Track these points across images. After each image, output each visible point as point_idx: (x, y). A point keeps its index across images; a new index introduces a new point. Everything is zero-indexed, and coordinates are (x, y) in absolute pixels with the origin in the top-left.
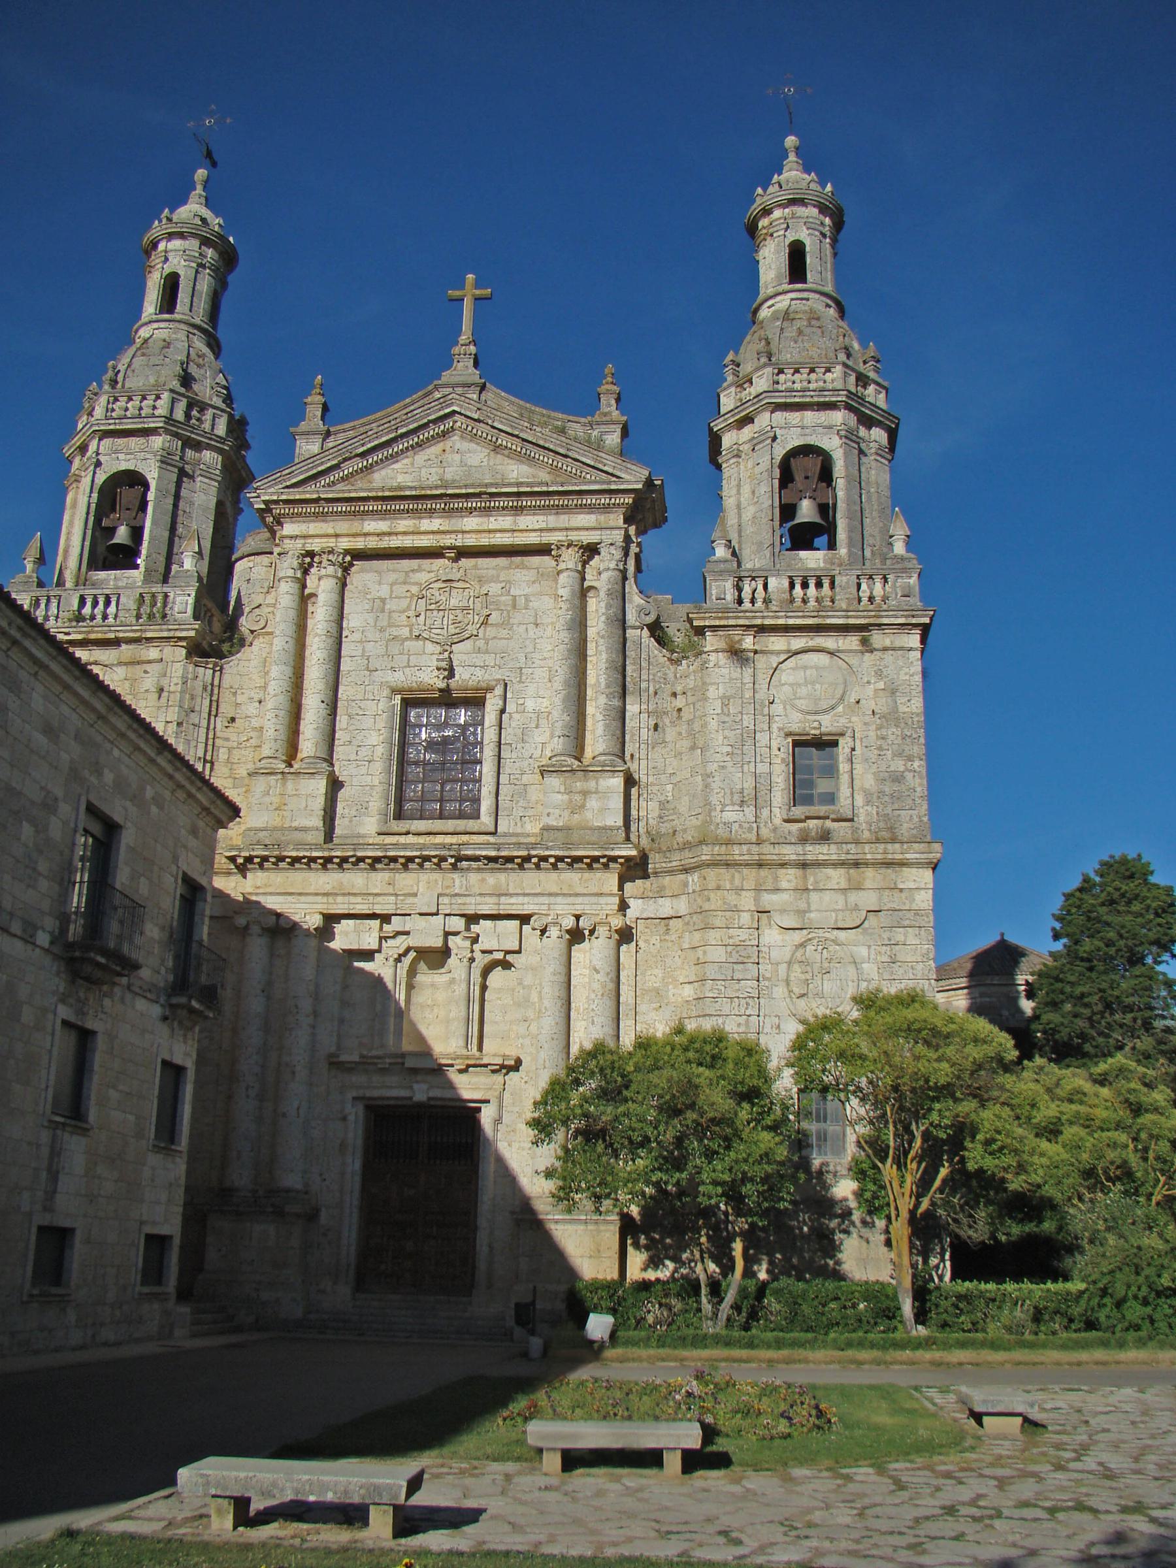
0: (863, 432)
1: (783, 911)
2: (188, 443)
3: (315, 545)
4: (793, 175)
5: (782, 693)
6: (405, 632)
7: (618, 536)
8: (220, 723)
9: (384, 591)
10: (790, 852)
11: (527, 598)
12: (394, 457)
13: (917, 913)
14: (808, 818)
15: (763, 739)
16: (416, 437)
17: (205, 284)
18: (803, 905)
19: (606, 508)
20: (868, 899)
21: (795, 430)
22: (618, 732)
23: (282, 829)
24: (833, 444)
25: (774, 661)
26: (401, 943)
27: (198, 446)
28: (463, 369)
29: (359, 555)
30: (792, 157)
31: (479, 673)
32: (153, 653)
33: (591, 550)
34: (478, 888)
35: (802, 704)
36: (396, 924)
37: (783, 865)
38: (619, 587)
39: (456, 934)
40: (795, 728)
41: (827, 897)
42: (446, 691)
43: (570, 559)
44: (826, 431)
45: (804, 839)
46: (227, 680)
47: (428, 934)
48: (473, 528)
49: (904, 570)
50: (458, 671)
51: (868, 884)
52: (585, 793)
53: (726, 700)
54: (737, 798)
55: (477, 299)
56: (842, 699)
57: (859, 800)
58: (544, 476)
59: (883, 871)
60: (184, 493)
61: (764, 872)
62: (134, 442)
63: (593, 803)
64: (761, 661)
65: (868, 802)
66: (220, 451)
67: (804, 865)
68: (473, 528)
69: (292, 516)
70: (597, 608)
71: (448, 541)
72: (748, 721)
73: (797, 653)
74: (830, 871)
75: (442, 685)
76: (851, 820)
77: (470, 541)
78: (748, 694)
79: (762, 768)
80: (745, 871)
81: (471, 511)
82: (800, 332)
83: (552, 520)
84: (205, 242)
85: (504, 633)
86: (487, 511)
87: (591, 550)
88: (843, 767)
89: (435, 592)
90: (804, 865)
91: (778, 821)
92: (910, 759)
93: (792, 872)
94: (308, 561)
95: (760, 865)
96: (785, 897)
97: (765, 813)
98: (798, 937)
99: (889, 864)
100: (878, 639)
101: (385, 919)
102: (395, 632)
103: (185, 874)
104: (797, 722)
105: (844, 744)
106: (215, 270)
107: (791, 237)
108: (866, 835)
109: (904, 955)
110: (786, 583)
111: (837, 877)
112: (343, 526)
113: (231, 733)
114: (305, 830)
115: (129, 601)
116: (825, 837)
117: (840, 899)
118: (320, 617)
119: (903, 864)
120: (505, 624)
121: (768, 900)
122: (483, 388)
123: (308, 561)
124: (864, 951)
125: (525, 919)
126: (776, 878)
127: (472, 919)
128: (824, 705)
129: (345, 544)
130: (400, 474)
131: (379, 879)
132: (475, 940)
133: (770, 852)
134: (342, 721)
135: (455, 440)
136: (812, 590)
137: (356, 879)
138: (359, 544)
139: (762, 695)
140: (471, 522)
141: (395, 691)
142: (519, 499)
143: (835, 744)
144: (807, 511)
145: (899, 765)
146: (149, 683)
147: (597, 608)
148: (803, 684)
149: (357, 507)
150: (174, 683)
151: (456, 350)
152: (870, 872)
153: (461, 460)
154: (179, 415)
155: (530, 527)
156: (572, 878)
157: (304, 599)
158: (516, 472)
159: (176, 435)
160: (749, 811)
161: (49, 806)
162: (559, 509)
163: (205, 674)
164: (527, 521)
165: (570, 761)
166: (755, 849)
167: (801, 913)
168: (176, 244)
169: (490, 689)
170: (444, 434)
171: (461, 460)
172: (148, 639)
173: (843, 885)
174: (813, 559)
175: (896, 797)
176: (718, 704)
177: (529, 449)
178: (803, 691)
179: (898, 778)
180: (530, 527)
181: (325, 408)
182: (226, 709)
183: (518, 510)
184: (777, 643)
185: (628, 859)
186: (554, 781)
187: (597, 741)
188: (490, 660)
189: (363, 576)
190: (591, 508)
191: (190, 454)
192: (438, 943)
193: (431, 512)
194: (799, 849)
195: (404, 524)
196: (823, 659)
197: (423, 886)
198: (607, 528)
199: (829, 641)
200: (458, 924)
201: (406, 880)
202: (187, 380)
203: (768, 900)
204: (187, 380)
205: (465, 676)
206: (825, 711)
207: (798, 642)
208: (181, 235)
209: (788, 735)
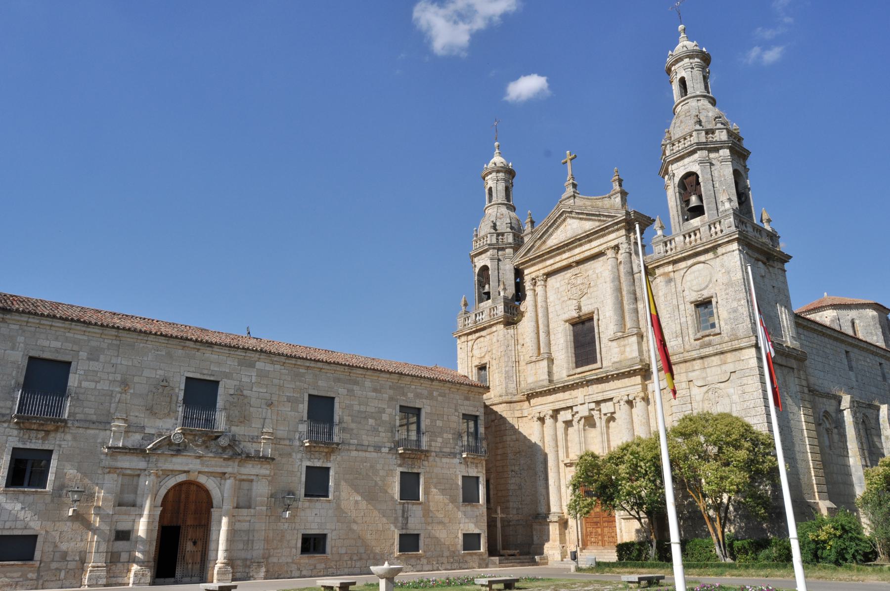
0: (712, 155)
1: (697, 379)
2: (499, 249)
3: (533, 275)
4: (685, 44)
5: (687, 285)
6: (566, 298)
7: (624, 239)
8: (519, 347)
9: (558, 285)
10: (695, 354)
11: (601, 273)
12: (551, 235)
13: (751, 369)
14: (703, 337)
15: (682, 307)
16: (554, 224)
17: (502, 186)
18: (704, 375)
19: (618, 230)
20: (730, 367)
21: (679, 170)
22: (635, 318)
23: (536, 382)
24: (696, 168)
25: (682, 272)
26: (577, 417)
27: (503, 249)
28: (570, 190)
29: (549, 275)
30: (683, 35)
31: (590, 306)
32: (494, 329)
33: (616, 248)
34: (596, 391)
35: (695, 288)
36: (575, 409)
37: (694, 360)
38: (628, 259)
39: (593, 409)
40: (693, 299)
41: (714, 369)
42: (579, 317)
43: (610, 253)
44: (691, 165)
45: (702, 347)
46: (520, 331)
47: (583, 411)
48: (579, 253)
49: (726, 216)
50: (583, 308)
51: (729, 360)
52: (624, 346)
53: (665, 296)
54: (674, 335)
55: (571, 160)
56: (710, 281)
57: (722, 323)
58: (597, 224)
59: (734, 353)
60: (501, 266)
61: (688, 364)
62: (483, 256)
63: (628, 349)
64: (678, 275)
65: (726, 324)
66: (511, 247)
67: (702, 358)
68: (579, 253)
69: (526, 268)
70: (622, 269)
71: (571, 260)
72: (675, 302)
73: (690, 267)
74: (713, 358)
75: (577, 315)
76: (720, 334)
77: (578, 258)
78: (673, 290)
79: (683, 320)
80: (681, 365)
81: (576, 247)
82: (681, 122)
83: (602, 240)
84: (498, 172)
85: (595, 289)
86: (581, 245)
87: (616, 248)
88: (715, 311)
89: (574, 281)
90: (702, 358)
91: (692, 341)
92: (739, 300)
93: (698, 361)
94: (534, 281)
95: (686, 362)
96: (697, 373)
97: (687, 338)
98: (705, 389)
99: (736, 350)
100: (720, 250)
101: (571, 408)
102: (563, 299)
103: (464, 415)
104: (695, 296)
105: (714, 301)
106: (506, 181)
107: (679, 77)
108: (727, 339)
109: (748, 389)
110: (682, 238)
111: (716, 360)
112: (540, 266)
113: (523, 350)
114: (543, 380)
115: (486, 312)
116: (709, 345)
117: (718, 369)
118: (540, 299)
119: (741, 349)
120: (596, 285)
121: (692, 375)
122: (575, 197)
123: (534, 281)
124: (731, 390)
125: (611, 399)
126: (693, 366)
127: (598, 403)
128: (703, 286)
129: (542, 272)
130: (553, 241)
131: (567, 395)
132: (600, 410)
133: (687, 356)
134: (552, 337)
135: (569, 221)
136: (693, 237)
137: (560, 396)
138: (546, 270)
139: (679, 289)
140: (577, 251)
141: (566, 321)
142: (589, 237)
143: (710, 302)
144: (694, 201)
145: (735, 304)
146: (495, 340)
147: (622, 269)
148: (696, 279)
149: (542, 258)
150: (501, 337)
151: (567, 183)
152: (729, 355)
153: (572, 228)
154: (494, 241)
155: (594, 246)
156: (626, 381)
157: (535, 295)
158: (590, 225)
159: (494, 248)
160: (680, 339)
161: (382, 411)
162: (603, 236)
163: (511, 331)
164: (595, 244)
165: (620, 334)
166: (681, 355)
167: (704, 378)
168: (490, 176)
169: (593, 313)
170: (564, 220)
171: (572, 228)
172: (493, 325)
173: (719, 363)
174: (696, 222)
175: (735, 319)
176: (663, 298)
177: (589, 216)
178: (695, 282)
179: (735, 311)
180: (594, 246)
181: (532, 223)
182: (521, 342)
183: (590, 241)
184: (683, 265)
185: (641, 369)
186: (614, 344)
187: (629, 324)
188: (593, 301)
189: (551, 281)
190: (613, 232)
191: (500, 253)
192: (586, 414)
193: (564, 252)
194: (698, 352)
195: (558, 258)
196: (702, 265)
197: (579, 394)
198: (617, 237)
199: (702, 258)
200: (593, 406)
201: (575, 393)
202: (494, 227)
203: (692, 375)
204: (494, 227)
205: (585, 310)
206: (704, 289)
207: (690, 262)
208: (490, 173)
209: (692, 303)
